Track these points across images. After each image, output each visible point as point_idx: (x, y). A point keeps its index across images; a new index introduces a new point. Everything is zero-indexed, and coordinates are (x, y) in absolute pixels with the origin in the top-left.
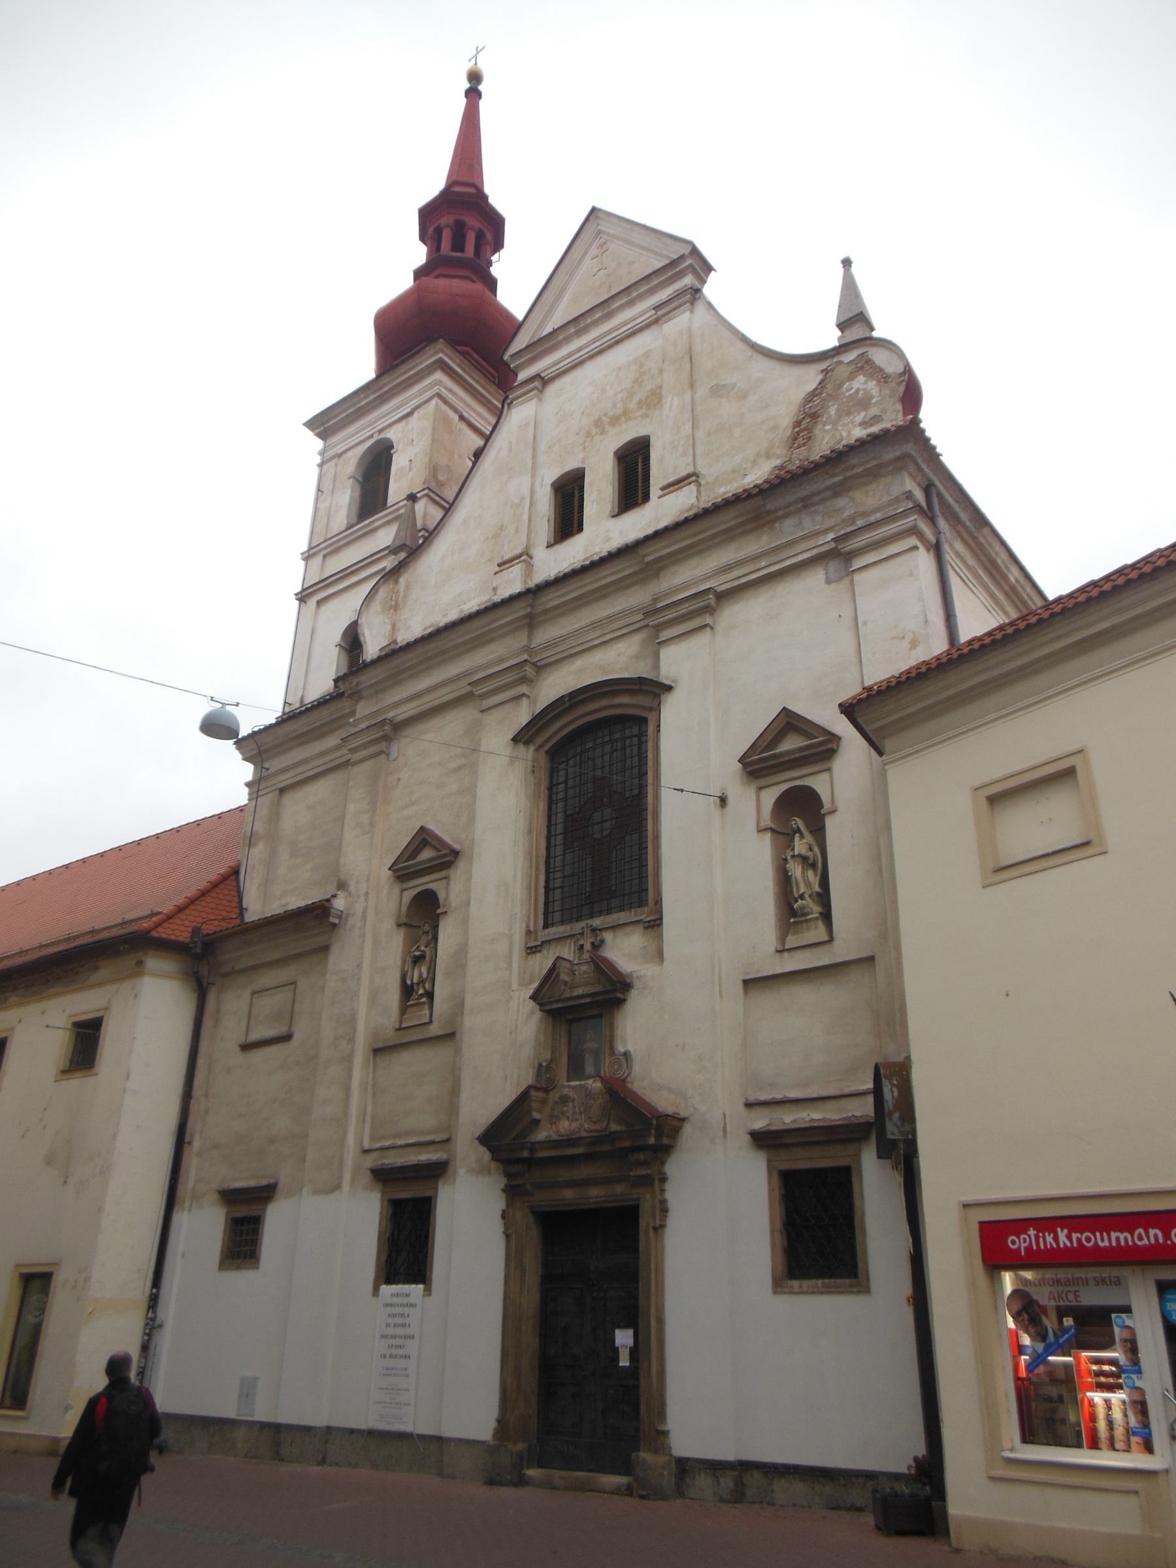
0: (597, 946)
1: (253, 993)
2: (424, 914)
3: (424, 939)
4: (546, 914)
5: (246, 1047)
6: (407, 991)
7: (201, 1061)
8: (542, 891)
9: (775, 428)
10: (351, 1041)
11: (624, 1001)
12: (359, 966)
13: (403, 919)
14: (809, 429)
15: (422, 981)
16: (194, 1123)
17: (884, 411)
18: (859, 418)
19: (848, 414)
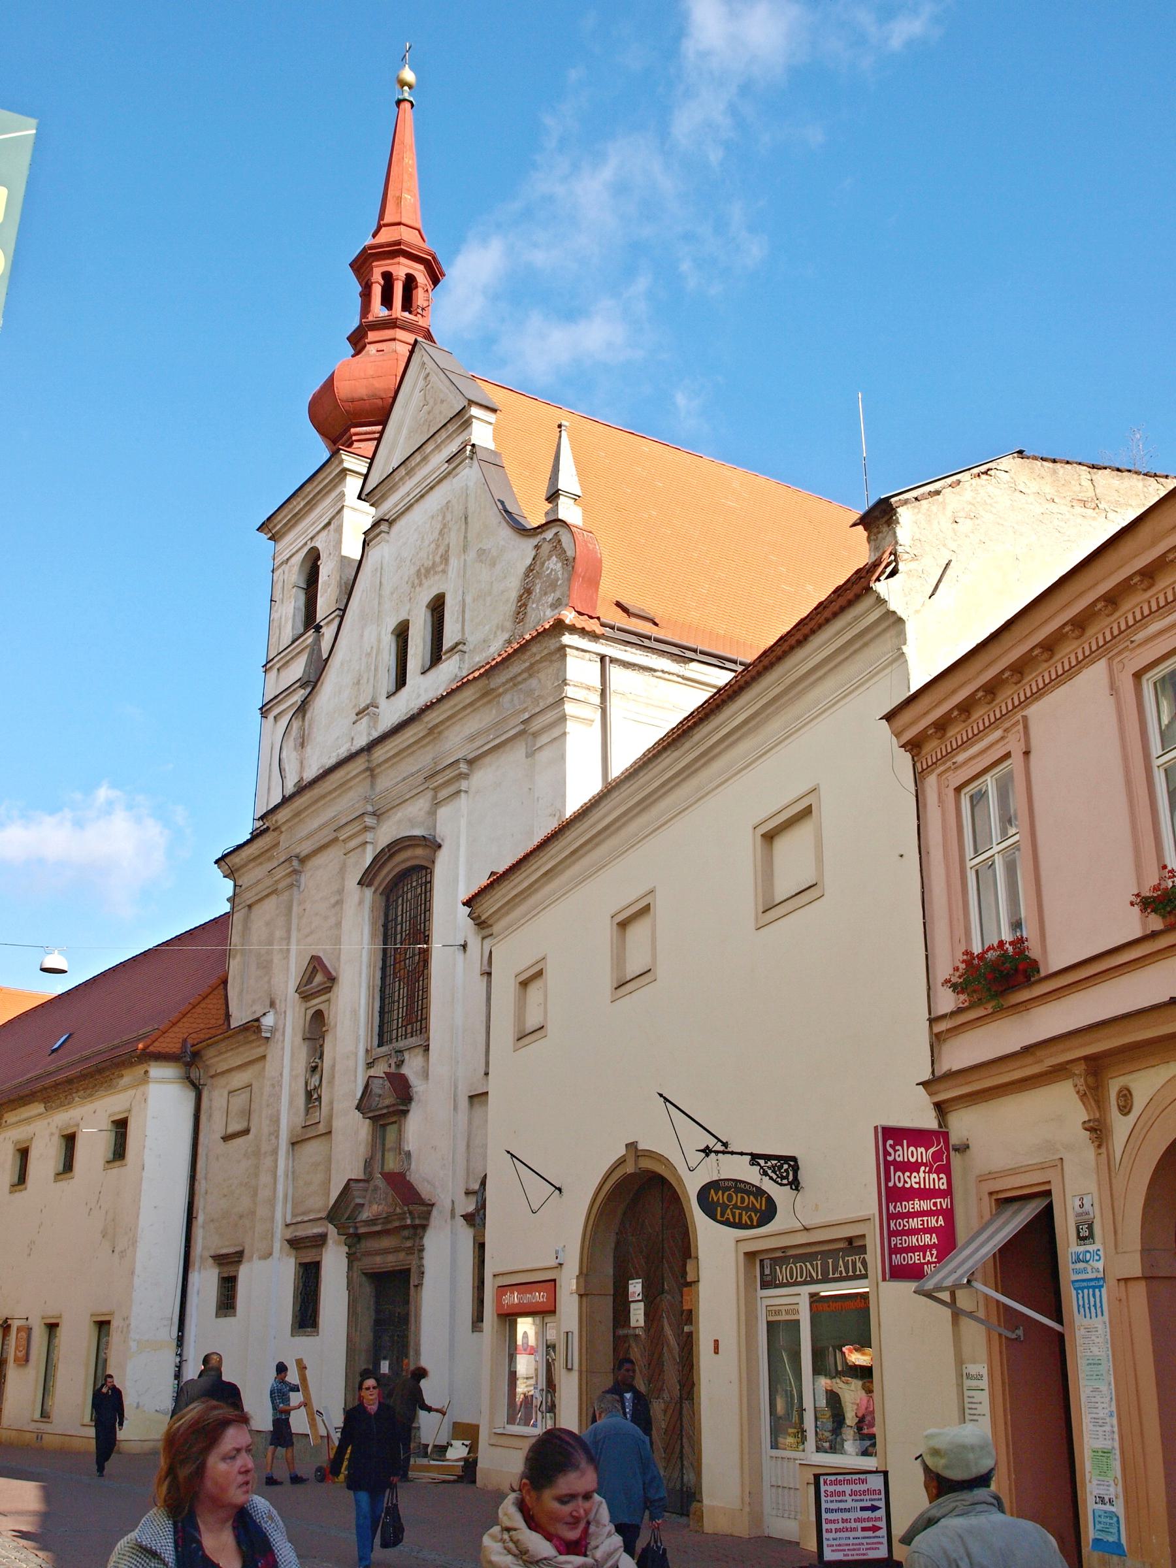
0: (400, 1064)
1: (230, 1093)
2: (317, 1028)
3: (318, 1055)
4: (381, 1035)
5: (226, 1138)
6: (309, 1094)
7: (201, 1151)
8: (377, 1015)
9: (508, 600)
10: (277, 1137)
11: (408, 1111)
12: (281, 1075)
13: (308, 1036)
14: (525, 605)
15: (315, 1088)
16: (199, 1203)
17: (563, 595)
18: (550, 599)
19: (545, 594)
